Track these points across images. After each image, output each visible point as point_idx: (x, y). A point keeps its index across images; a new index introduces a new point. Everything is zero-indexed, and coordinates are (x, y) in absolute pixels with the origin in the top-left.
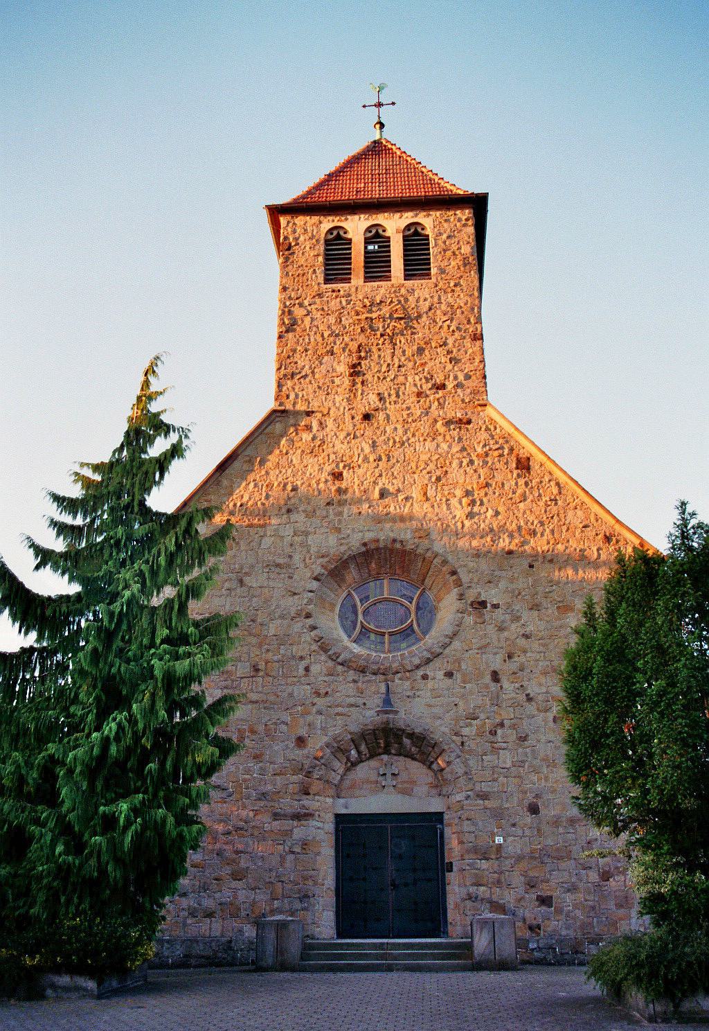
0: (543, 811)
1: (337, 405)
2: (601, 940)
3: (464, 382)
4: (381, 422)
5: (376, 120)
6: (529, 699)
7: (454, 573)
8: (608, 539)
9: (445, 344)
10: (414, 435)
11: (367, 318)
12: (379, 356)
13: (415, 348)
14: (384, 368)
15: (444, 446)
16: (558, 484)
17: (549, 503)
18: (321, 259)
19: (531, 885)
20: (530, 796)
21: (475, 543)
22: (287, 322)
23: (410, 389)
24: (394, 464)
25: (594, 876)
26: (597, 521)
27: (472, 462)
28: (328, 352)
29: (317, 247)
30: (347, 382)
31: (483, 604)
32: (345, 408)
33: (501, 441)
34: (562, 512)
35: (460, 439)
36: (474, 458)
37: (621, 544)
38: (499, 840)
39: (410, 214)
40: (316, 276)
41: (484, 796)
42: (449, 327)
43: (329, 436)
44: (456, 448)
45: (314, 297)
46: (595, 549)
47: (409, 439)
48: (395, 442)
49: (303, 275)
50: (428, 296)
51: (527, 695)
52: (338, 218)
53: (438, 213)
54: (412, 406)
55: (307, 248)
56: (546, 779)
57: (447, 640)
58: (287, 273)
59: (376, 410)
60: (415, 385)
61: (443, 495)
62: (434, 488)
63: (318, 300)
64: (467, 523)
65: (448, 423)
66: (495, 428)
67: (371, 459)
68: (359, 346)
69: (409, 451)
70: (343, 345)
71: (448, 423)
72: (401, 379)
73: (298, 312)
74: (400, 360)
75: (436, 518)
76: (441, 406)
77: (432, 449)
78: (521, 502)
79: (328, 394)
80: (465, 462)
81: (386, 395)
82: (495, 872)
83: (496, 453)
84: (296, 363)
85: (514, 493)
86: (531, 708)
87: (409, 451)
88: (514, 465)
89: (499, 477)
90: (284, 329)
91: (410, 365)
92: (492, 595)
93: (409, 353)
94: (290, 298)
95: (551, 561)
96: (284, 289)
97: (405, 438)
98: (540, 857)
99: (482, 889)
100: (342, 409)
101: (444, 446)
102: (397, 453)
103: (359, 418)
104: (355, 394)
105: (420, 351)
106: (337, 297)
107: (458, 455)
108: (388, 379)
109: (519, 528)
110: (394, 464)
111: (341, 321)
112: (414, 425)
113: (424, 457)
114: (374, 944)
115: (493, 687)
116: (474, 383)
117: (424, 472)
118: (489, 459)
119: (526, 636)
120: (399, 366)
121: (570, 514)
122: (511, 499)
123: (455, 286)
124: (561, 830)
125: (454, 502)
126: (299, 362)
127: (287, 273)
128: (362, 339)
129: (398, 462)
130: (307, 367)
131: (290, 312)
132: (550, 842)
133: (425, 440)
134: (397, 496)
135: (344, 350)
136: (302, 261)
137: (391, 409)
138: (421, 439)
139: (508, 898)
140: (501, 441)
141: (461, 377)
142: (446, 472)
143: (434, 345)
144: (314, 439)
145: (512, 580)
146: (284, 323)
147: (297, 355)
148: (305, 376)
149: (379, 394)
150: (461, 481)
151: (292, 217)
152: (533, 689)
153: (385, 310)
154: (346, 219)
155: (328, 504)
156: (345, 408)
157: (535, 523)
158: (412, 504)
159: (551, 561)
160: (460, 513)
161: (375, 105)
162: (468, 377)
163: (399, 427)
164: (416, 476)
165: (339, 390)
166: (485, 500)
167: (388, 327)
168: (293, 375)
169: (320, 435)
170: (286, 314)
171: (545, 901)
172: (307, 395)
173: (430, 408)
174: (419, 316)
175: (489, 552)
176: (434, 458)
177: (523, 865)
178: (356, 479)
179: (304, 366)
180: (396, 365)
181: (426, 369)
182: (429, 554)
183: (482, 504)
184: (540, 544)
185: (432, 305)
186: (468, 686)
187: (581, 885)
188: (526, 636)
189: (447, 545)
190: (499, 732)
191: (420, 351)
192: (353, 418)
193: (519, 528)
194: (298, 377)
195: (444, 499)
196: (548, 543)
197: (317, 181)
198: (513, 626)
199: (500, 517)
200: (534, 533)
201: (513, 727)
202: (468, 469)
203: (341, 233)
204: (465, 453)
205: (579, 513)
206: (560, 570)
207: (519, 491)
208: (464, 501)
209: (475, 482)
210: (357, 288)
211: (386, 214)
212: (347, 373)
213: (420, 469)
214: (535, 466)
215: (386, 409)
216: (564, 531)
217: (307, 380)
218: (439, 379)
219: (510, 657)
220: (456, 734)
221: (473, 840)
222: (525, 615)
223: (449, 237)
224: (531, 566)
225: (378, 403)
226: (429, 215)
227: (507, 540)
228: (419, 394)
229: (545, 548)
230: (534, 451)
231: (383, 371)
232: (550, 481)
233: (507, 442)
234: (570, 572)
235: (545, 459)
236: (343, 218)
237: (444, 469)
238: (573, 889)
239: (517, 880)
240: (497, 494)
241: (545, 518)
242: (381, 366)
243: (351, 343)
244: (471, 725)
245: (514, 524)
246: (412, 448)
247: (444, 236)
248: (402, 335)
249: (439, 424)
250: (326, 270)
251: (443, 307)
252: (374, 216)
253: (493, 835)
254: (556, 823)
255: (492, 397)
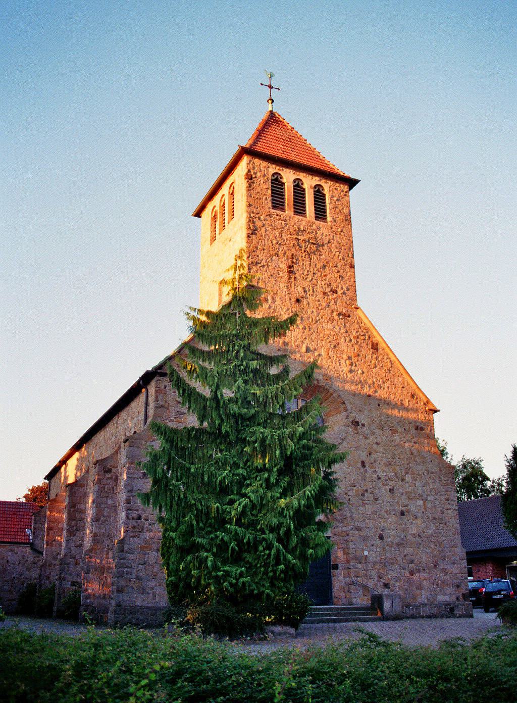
0: (385, 539)
1: (281, 289)
2: (411, 606)
3: (346, 292)
4: (305, 305)
5: (268, 98)
6: (379, 478)
7: (344, 403)
8: (413, 396)
9: (336, 266)
10: (322, 318)
11: (296, 238)
12: (303, 264)
13: (322, 264)
14: (306, 273)
15: (337, 328)
16: (391, 361)
17: (387, 371)
18: (269, 192)
19: (380, 578)
20: (379, 530)
21: (353, 388)
22: (252, 228)
23: (319, 289)
24: (312, 333)
25: (407, 574)
26: (408, 385)
27: (351, 340)
28: (276, 254)
29: (267, 183)
30: (286, 276)
31: (357, 423)
32: (285, 292)
33: (364, 331)
34: (392, 377)
35: (345, 326)
36: (352, 338)
37: (418, 399)
38: (366, 553)
39: (317, 178)
40: (268, 202)
41: (359, 529)
42: (339, 256)
43: (278, 308)
44: (343, 331)
45: (267, 216)
46: (407, 400)
47: (320, 320)
48: (312, 320)
49: (260, 199)
50: (327, 234)
51: (378, 476)
52: (278, 167)
53: (332, 183)
54: (321, 299)
55: (262, 182)
56: (386, 521)
57: (341, 441)
58: (251, 195)
59: (302, 298)
60: (322, 287)
61: (337, 357)
62: (333, 352)
63: (268, 218)
64: (349, 375)
65: (339, 314)
66: (362, 323)
67: (301, 327)
68: (292, 255)
69: (320, 327)
70: (283, 252)
71: (339, 314)
72: (314, 281)
73: (259, 223)
74: (314, 270)
75: (334, 370)
76: (335, 303)
77: (332, 328)
78: (374, 368)
79: (276, 281)
80: (347, 340)
81: (307, 289)
82: (365, 570)
83: (362, 338)
84: (258, 256)
85: (371, 362)
86: (380, 483)
87: (320, 327)
88: (371, 347)
89: (363, 352)
90: (250, 232)
91: (319, 274)
92: (362, 419)
93: (318, 266)
94: (253, 213)
95: (388, 404)
96: (250, 205)
97: (318, 319)
98: (384, 563)
99: (359, 579)
100: (284, 292)
101: (337, 328)
102: (313, 326)
103: (293, 300)
104: (291, 284)
105: (324, 267)
106: (279, 219)
107: (344, 334)
108: (308, 280)
109: (373, 383)
110: (312, 333)
111: (282, 236)
112: (322, 311)
113: (327, 332)
114: (327, 608)
115: (362, 469)
116: (350, 293)
117: (328, 341)
118: (359, 340)
119: (377, 444)
120: (314, 274)
121: (396, 379)
122: (369, 365)
123: (341, 231)
124: (393, 549)
125: (342, 361)
126: (260, 256)
127: (251, 195)
128: (293, 250)
129: (314, 332)
130: (264, 260)
131: (253, 222)
132: (388, 555)
133: (328, 322)
134: (314, 353)
135: (284, 254)
136: (259, 190)
137: (310, 299)
138: (326, 321)
139: (371, 584)
140: (364, 331)
141: (345, 288)
142: (338, 343)
143: (331, 264)
144: (270, 307)
145: (370, 411)
146: (250, 228)
147: (258, 251)
148: (263, 266)
149: (304, 288)
150: (346, 350)
151: (253, 158)
152: (380, 474)
153: (306, 237)
154: (283, 170)
155: (279, 350)
156: (285, 292)
157: (381, 381)
158: (322, 359)
159: (388, 404)
160: (346, 369)
161: (268, 86)
162: (348, 289)
163: (314, 311)
164: (323, 342)
165: (282, 280)
166: (357, 363)
167: (307, 247)
168: (257, 263)
169: (273, 306)
170: (251, 222)
171: (386, 586)
172: (265, 278)
173: (330, 303)
174: (323, 245)
175: (360, 394)
176: (332, 334)
177: (377, 566)
178: (293, 338)
179: (262, 259)
180: (312, 272)
181: (327, 279)
182: (331, 390)
183: (356, 366)
184: (382, 394)
185: (330, 240)
186: (350, 467)
187: (402, 578)
188: (377, 444)
189: (340, 386)
190: (366, 494)
191: (324, 267)
192: (290, 299)
193: (373, 383)
194: (259, 265)
195: (338, 359)
196: (387, 394)
197: (347, 174)
198: (371, 438)
199: (364, 375)
200: (380, 387)
201: (372, 493)
202: (349, 344)
203: (279, 177)
204: (347, 334)
205: (400, 379)
206: (392, 409)
207: (373, 362)
208: (347, 361)
209: (352, 352)
210: (290, 217)
211: (304, 174)
212: (286, 271)
213: (325, 338)
214: (380, 350)
215: (307, 298)
216: (394, 388)
217: (265, 269)
218: (334, 287)
219: (370, 454)
220: (346, 494)
221: (354, 552)
222: (377, 432)
223: (337, 200)
224: (379, 405)
225: (303, 293)
226: (327, 183)
227: (368, 389)
228: (324, 293)
229: (385, 396)
230: (380, 340)
231: (305, 274)
232: (387, 359)
233: (367, 332)
234: (396, 412)
235: (386, 346)
236: (281, 169)
237: (337, 341)
238: (398, 580)
239: (375, 575)
240: (363, 361)
241: (385, 379)
242: (304, 271)
243: (288, 252)
244: (352, 490)
245: (371, 380)
246: (321, 325)
247: (335, 198)
248: (315, 254)
249: (335, 314)
250: (272, 199)
251: (335, 243)
252: (298, 173)
253: (363, 550)
254: (391, 545)
255: (359, 303)
